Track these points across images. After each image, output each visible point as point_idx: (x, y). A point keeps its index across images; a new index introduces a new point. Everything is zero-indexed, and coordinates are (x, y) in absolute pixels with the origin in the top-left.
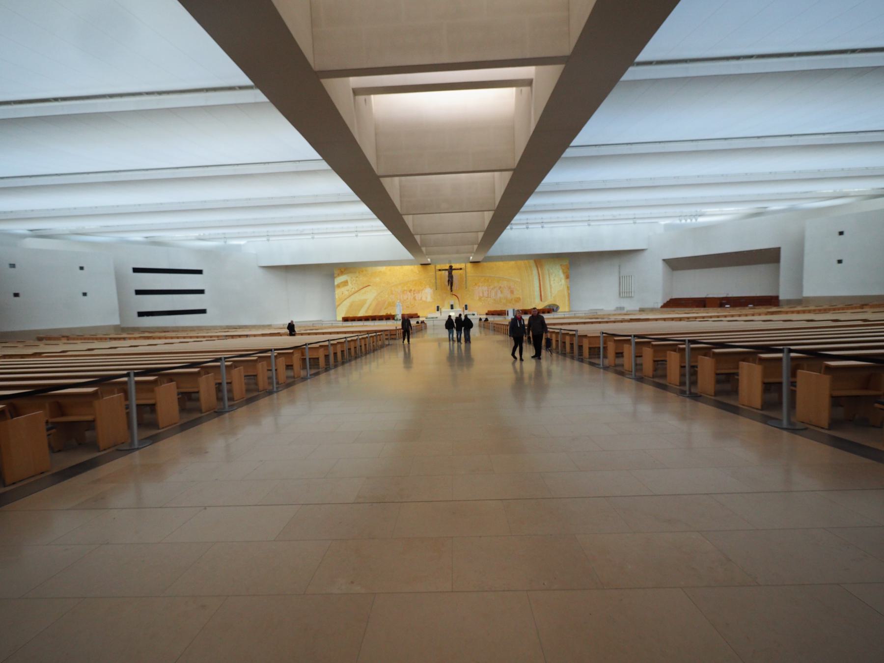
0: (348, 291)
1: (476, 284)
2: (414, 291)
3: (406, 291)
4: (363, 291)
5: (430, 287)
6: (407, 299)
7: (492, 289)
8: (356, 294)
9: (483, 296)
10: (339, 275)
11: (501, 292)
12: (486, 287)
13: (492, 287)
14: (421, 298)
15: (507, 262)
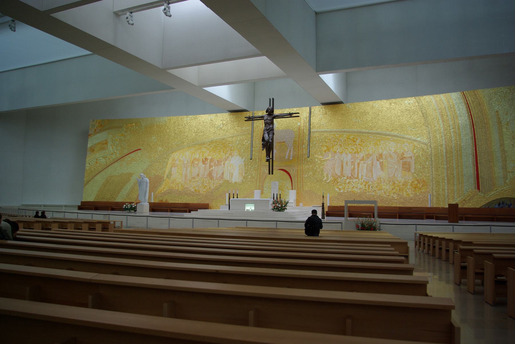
0: (105, 157)
1: (329, 150)
2: (212, 160)
3: (198, 160)
4: (127, 158)
5: (240, 155)
6: (198, 175)
7: (363, 159)
8: (116, 164)
9: (342, 175)
10: (96, 132)
11: (382, 168)
12: (350, 156)
13: (361, 155)
14: (223, 174)
15: (399, 100)
